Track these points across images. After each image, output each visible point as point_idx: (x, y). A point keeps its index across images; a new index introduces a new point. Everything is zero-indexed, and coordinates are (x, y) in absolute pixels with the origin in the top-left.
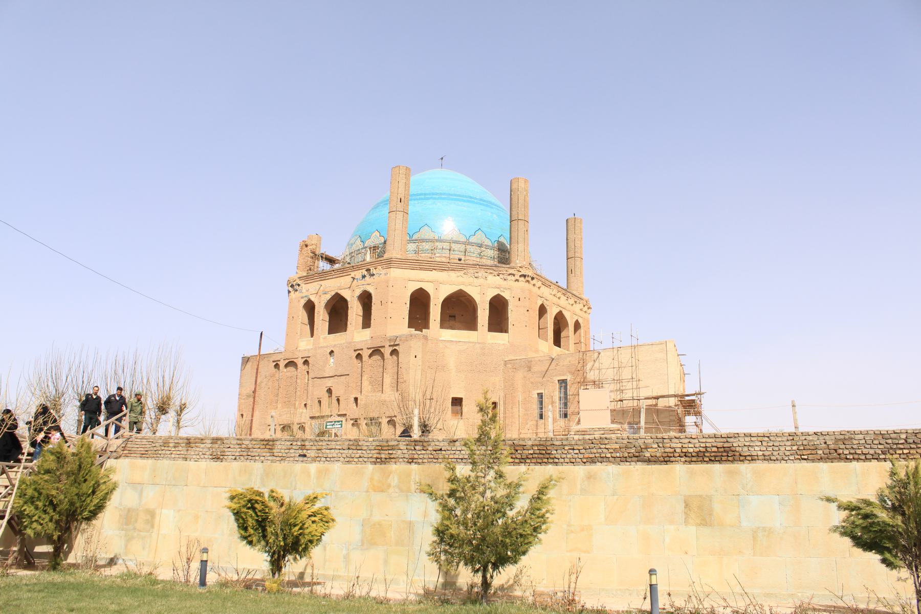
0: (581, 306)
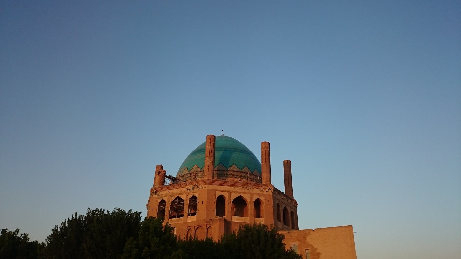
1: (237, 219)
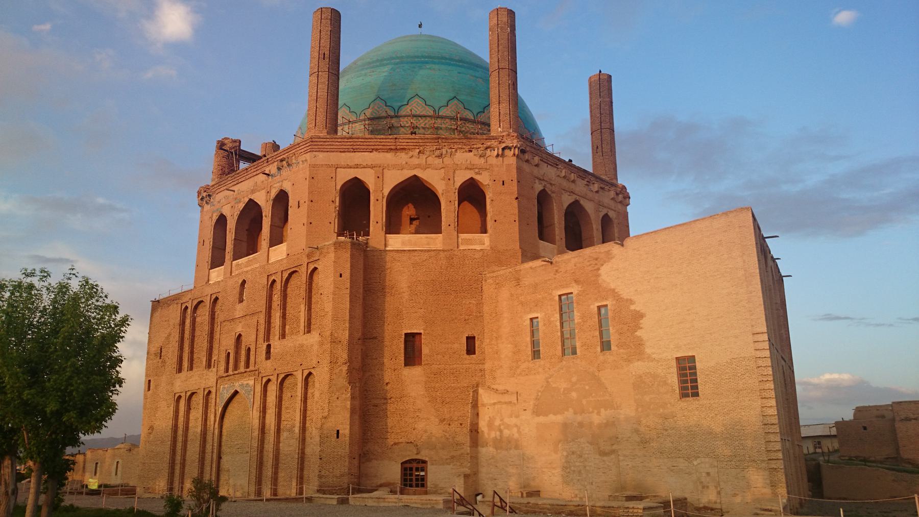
0: (612, 194)
1: (403, 243)
